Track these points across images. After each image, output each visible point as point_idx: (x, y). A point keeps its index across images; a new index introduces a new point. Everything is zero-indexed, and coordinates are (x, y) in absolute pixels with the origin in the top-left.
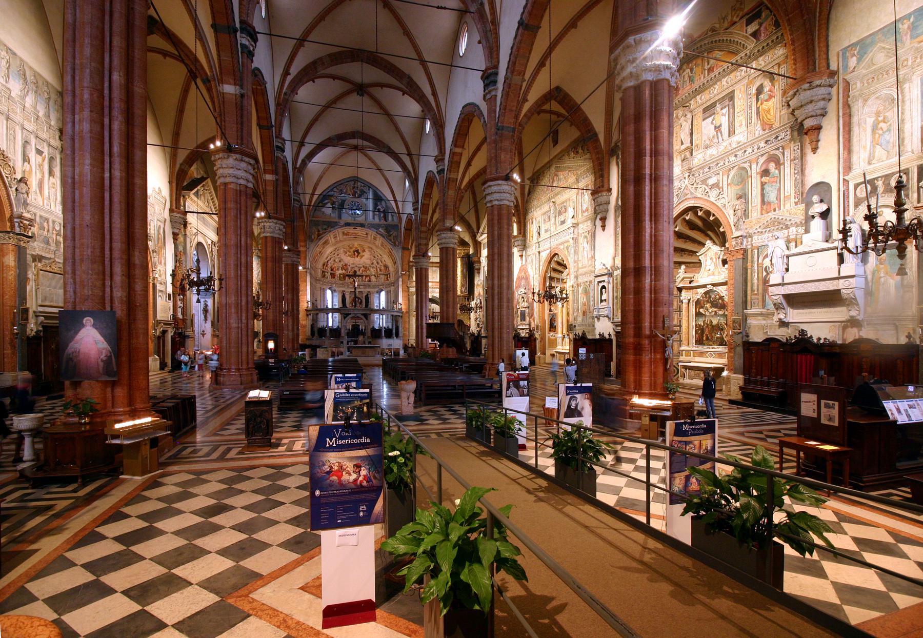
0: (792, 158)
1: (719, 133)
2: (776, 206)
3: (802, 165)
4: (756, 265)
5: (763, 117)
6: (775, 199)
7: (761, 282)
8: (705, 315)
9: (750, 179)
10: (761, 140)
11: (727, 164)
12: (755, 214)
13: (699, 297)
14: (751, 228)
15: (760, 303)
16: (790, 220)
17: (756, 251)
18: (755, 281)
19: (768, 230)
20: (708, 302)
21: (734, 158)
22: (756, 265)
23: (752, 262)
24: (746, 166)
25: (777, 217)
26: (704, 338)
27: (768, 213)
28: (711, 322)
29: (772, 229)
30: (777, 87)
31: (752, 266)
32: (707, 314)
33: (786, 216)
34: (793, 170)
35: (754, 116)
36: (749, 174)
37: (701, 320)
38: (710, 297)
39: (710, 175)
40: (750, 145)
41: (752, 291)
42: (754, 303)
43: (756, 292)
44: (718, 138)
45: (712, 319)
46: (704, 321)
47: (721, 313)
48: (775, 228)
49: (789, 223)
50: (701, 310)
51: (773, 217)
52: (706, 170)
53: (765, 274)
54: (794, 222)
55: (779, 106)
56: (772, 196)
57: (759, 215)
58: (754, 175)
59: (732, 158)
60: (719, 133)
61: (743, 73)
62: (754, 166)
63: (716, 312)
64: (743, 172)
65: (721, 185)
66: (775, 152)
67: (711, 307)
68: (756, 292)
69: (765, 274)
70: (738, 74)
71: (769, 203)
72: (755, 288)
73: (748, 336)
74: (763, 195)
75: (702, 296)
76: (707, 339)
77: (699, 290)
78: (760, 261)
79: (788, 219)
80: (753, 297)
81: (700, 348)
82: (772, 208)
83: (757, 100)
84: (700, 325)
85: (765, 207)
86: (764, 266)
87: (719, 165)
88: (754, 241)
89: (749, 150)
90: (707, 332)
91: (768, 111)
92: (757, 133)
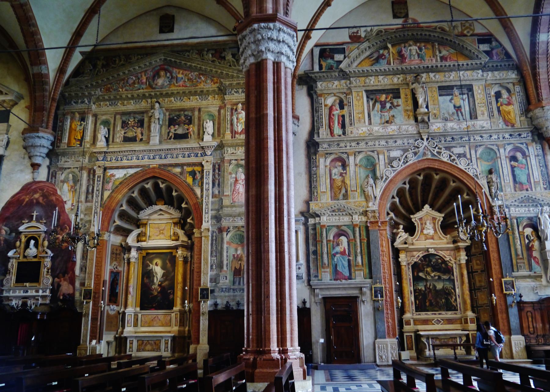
0: (536, 154)
1: (459, 112)
2: (528, 187)
3: (545, 162)
4: (517, 233)
5: (504, 116)
6: (526, 181)
7: (524, 248)
8: (426, 280)
9: (499, 160)
10: (508, 132)
11: (472, 140)
12: (509, 190)
13: (415, 260)
14: (506, 200)
15: (527, 266)
16: (543, 201)
17: (515, 221)
18: (519, 247)
19: (523, 205)
20: (428, 266)
21: (480, 138)
22: (517, 233)
23: (513, 229)
24: (495, 148)
25: (530, 196)
26: (427, 304)
27: (521, 191)
28: (435, 287)
29: (527, 204)
30: (514, 98)
31: (513, 233)
32: (429, 278)
33: (538, 196)
34: (538, 164)
35: (496, 112)
36: (498, 155)
37: (421, 284)
38: (430, 261)
39: (454, 145)
40: (497, 132)
41: (517, 255)
42: (521, 266)
43: (521, 257)
44: (458, 115)
45: (436, 284)
46: (425, 286)
47: (446, 277)
48: (531, 204)
49: (542, 203)
50: (421, 274)
51: (527, 195)
52: (449, 139)
53: (527, 241)
54: (546, 203)
55: (518, 112)
56: (523, 178)
57: (513, 190)
58: (503, 157)
59: (478, 138)
60: (459, 112)
61: (479, 76)
62: (502, 150)
63: (439, 278)
64: (492, 153)
65: (468, 156)
66: (519, 145)
67: (433, 271)
68: (521, 257)
69: (527, 241)
70: (475, 74)
71: (521, 184)
72: (520, 252)
73: (521, 296)
74: (514, 176)
75: (420, 260)
76: (431, 304)
77: (415, 253)
78: (521, 229)
79: (541, 199)
80: (518, 261)
81: (423, 315)
82: (525, 187)
83: (497, 102)
84: (421, 290)
85: (517, 185)
86: (526, 235)
87: (464, 139)
88: (511, 212)
89: (495, 137)
90: (430, 297)
91: (509, 113)
92: (500, 125)
